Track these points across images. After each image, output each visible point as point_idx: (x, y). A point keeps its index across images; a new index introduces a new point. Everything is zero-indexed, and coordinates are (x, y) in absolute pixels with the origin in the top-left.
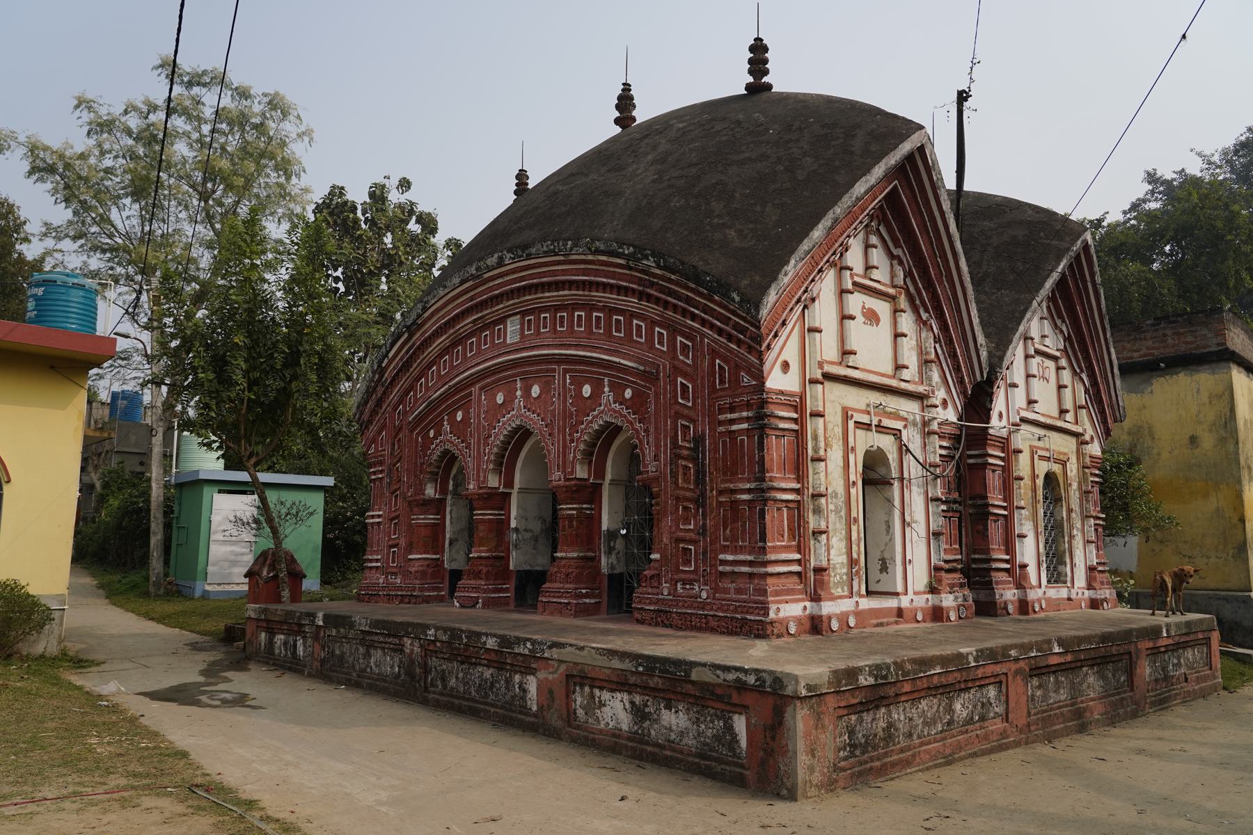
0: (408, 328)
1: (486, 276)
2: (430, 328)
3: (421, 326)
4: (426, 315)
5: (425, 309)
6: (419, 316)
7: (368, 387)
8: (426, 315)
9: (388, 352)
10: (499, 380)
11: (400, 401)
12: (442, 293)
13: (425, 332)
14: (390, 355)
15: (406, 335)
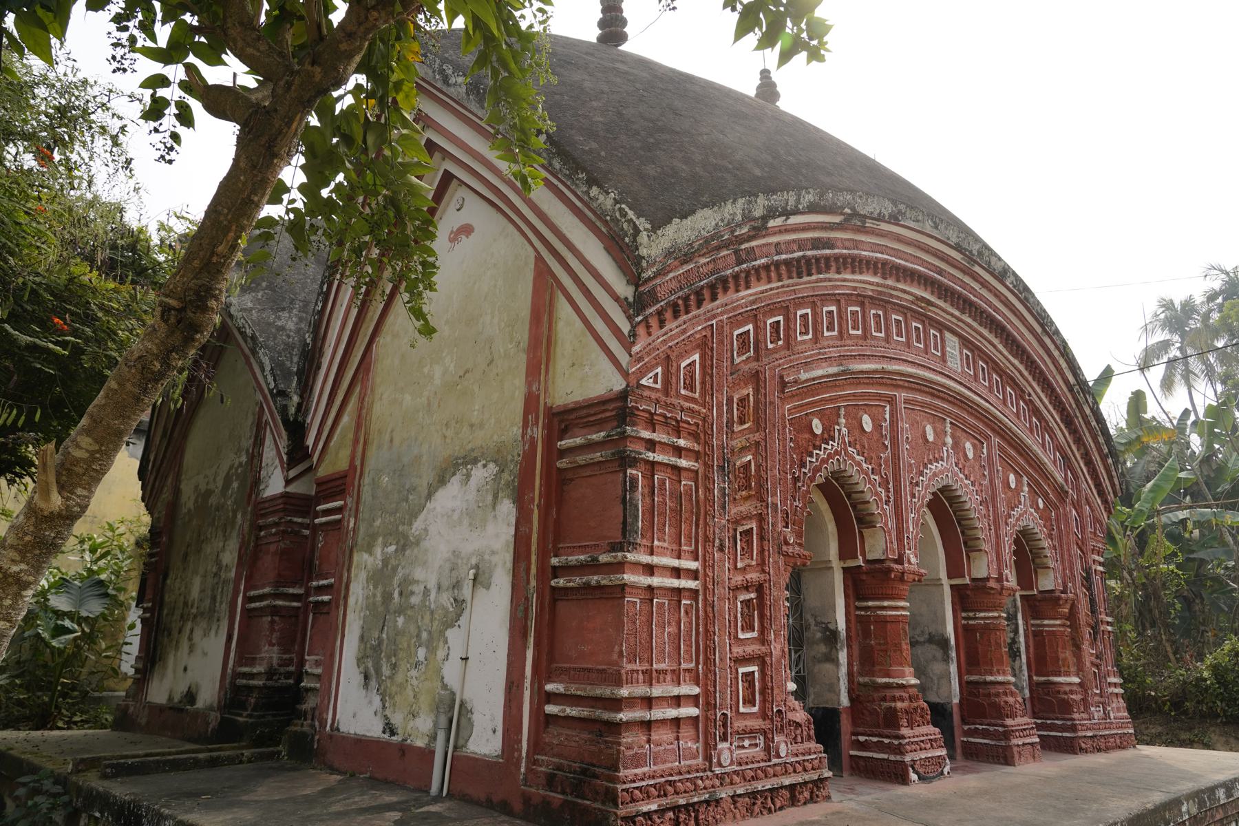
0: (855, 214)
1: (977, 269)
2: (868, 247)
3: (862, 230)
4: (884, 226)
5: (894, 219)
6: (880, 218)
7: (716, 235)
8: (884, 226)
9: (796, 212)
10: (930, 406)
11: (754, 317)
12: (929, 230)
13: (856, 244)
14: (794, 220)
15: (837, 219)
